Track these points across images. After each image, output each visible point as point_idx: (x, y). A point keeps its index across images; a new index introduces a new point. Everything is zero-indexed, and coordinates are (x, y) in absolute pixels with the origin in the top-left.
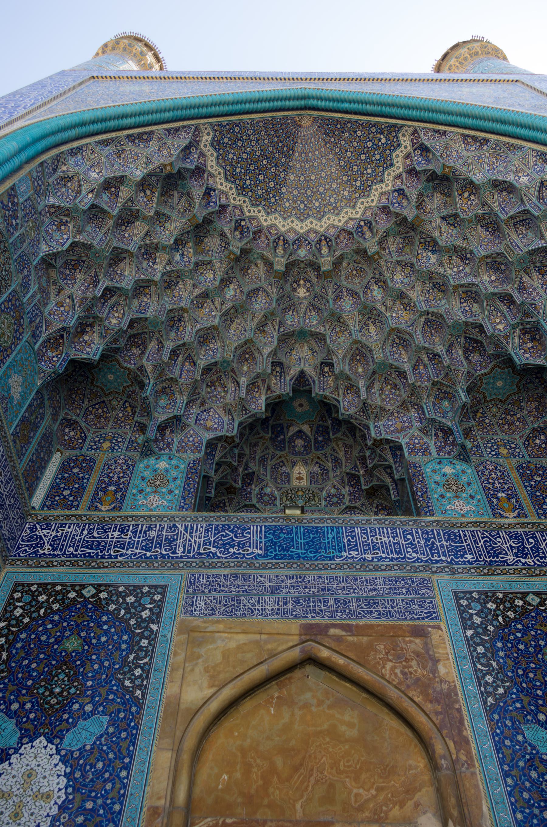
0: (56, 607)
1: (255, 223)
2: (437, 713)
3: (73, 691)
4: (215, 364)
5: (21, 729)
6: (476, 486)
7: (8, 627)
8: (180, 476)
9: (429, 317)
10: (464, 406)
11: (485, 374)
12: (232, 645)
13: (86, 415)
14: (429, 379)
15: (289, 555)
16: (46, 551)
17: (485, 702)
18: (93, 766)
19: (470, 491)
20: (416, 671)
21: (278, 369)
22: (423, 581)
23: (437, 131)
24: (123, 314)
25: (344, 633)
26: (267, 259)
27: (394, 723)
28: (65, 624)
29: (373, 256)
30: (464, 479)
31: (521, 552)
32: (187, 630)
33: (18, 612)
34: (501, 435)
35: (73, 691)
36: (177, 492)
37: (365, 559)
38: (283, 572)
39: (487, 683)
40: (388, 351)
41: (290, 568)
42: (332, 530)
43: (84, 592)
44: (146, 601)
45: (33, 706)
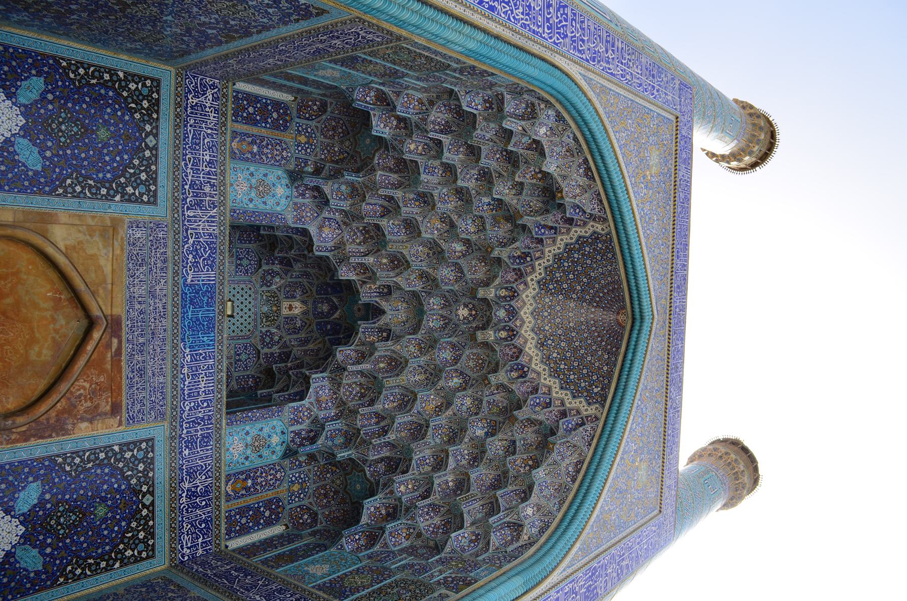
1: (529, 269)
2: (48, 419)
3: (63, 139)
4: (384, 235)
5: (31, 104)
6: (258, 462)
7: (120, 80)
8: (267, 207)
9: (425, 428)
10: (334, 456)
11: (365, 475)
12: (102, 262)
13: (334, 119)
14: (363, 426)
15: (186, 305)
17: (58, 456)
19: (253, 456)
20: (82, 405)
21: (386, 290)
22: (163, 415)
23: (592, 439)
24: (421, 154)
25: (113, 350)
26: (493, 281)
28: (121, 126)
29: (487, 378)
30: (265, 452)
31: (192, 494)
32: (115, 225)
33: (133, 86)
34: (314, 487)
35: (63, 139)
36: (251, 206)
37: (182, 367)
38: (170, 300)
39: (74, 458)
40: (397, 391)
41: (173, 306)
43: (151, 137)
44: (142, 189)
45: (50, 111)
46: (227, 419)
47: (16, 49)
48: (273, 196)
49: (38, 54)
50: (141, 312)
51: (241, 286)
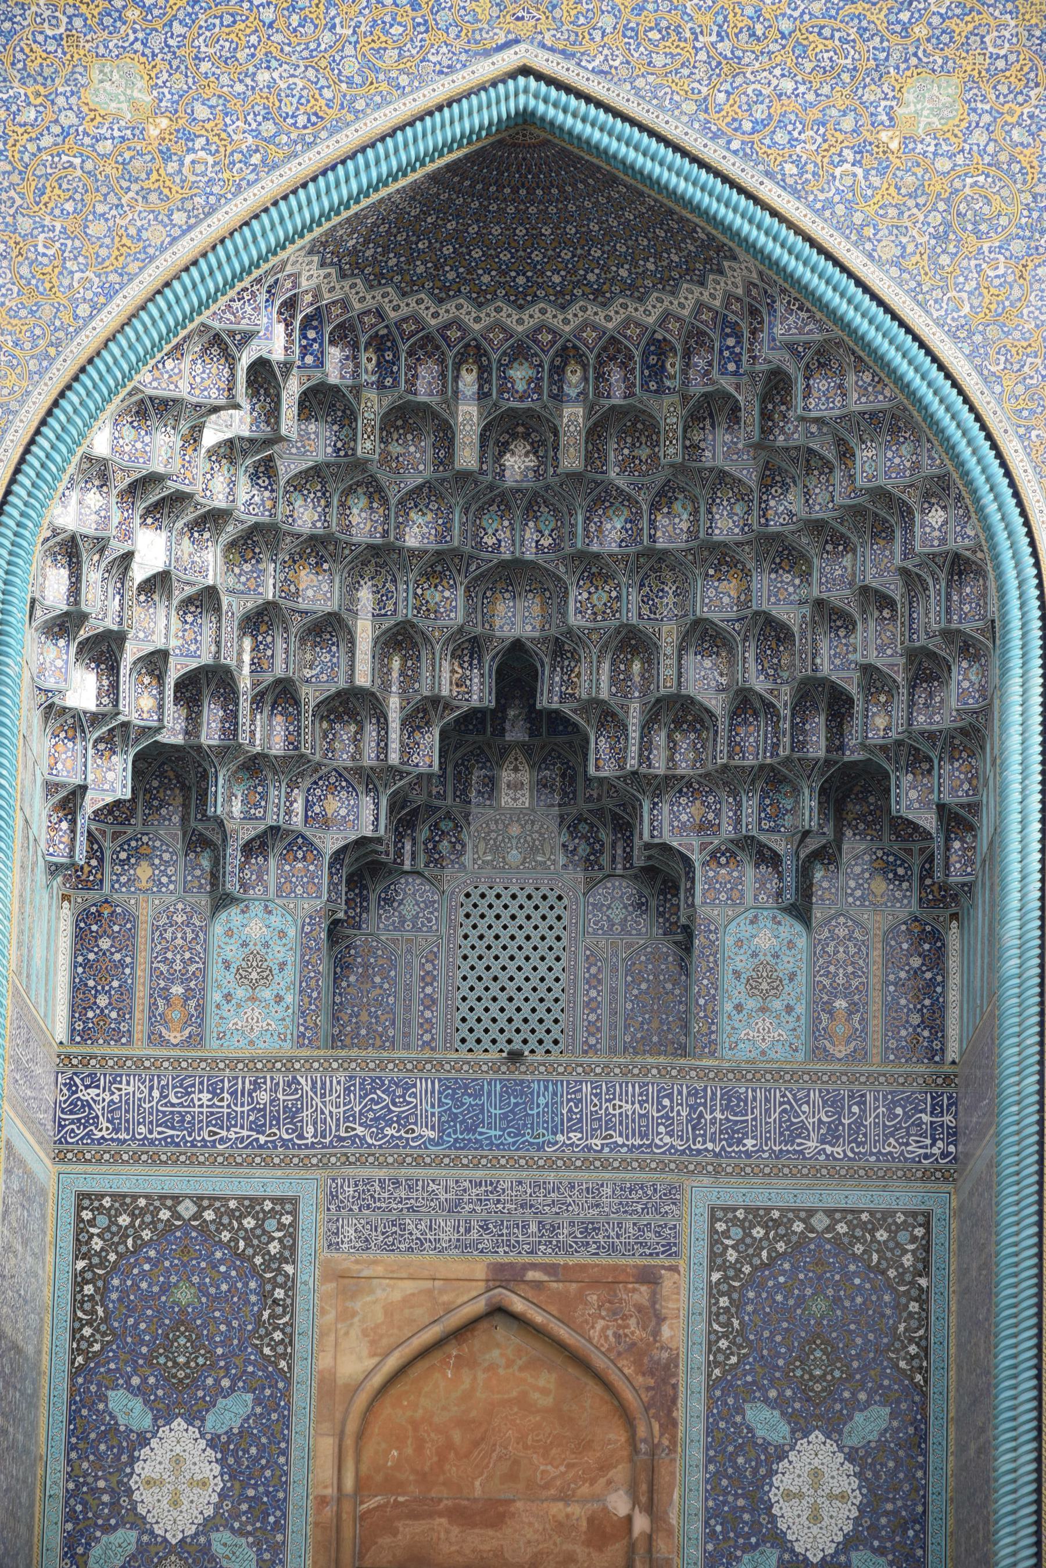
0: (146, 1234)
1: (409, 327)
2: (648, 1389)
6: (801, 978)
7: (91, 1267)
8: (290, 960)
12: (397, 1296)
16: (104, 1133)
17: (709, 1375)
18: (246, 1451)
25: (546, 1278)
27: (599, 1390)
28: (167, 1264)
30: (787, 964)
31: (831, 1134)
35: (201, 1361)
36: (289, 999)
37: (589, 1148)
39: (719, 1350)
41: (476, 1166)
42: (546, 1088)
44: (271, 1225)
46: (701, 1057)
47: (71, 1434)
48: (266, 945)
49: (72, 1401)
50: (485, 1228)
51: (461, 918)
